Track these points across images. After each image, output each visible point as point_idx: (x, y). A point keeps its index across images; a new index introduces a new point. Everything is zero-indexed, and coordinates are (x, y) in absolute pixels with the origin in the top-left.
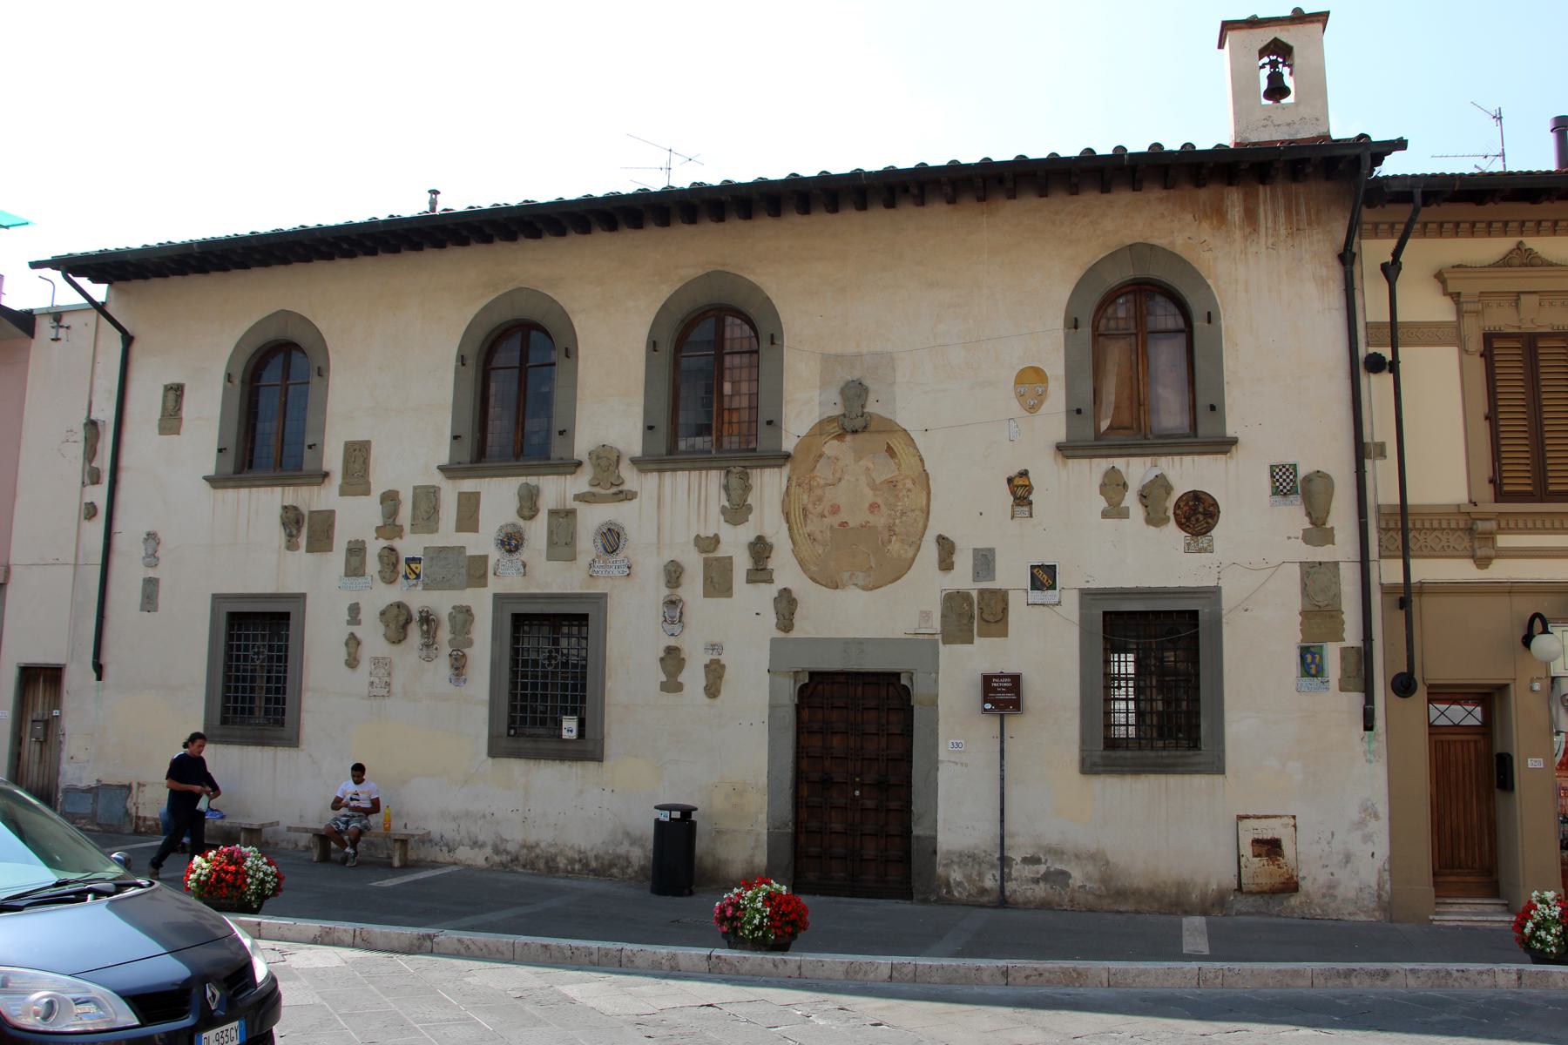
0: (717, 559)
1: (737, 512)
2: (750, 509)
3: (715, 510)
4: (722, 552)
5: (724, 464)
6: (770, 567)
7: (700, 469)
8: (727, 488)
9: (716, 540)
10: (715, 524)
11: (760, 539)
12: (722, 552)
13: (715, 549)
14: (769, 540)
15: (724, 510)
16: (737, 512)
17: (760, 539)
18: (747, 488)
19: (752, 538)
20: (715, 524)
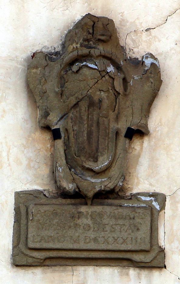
6: (142, 182)
11: (95, 35)
14: (137, 46)
17: (95, 35)
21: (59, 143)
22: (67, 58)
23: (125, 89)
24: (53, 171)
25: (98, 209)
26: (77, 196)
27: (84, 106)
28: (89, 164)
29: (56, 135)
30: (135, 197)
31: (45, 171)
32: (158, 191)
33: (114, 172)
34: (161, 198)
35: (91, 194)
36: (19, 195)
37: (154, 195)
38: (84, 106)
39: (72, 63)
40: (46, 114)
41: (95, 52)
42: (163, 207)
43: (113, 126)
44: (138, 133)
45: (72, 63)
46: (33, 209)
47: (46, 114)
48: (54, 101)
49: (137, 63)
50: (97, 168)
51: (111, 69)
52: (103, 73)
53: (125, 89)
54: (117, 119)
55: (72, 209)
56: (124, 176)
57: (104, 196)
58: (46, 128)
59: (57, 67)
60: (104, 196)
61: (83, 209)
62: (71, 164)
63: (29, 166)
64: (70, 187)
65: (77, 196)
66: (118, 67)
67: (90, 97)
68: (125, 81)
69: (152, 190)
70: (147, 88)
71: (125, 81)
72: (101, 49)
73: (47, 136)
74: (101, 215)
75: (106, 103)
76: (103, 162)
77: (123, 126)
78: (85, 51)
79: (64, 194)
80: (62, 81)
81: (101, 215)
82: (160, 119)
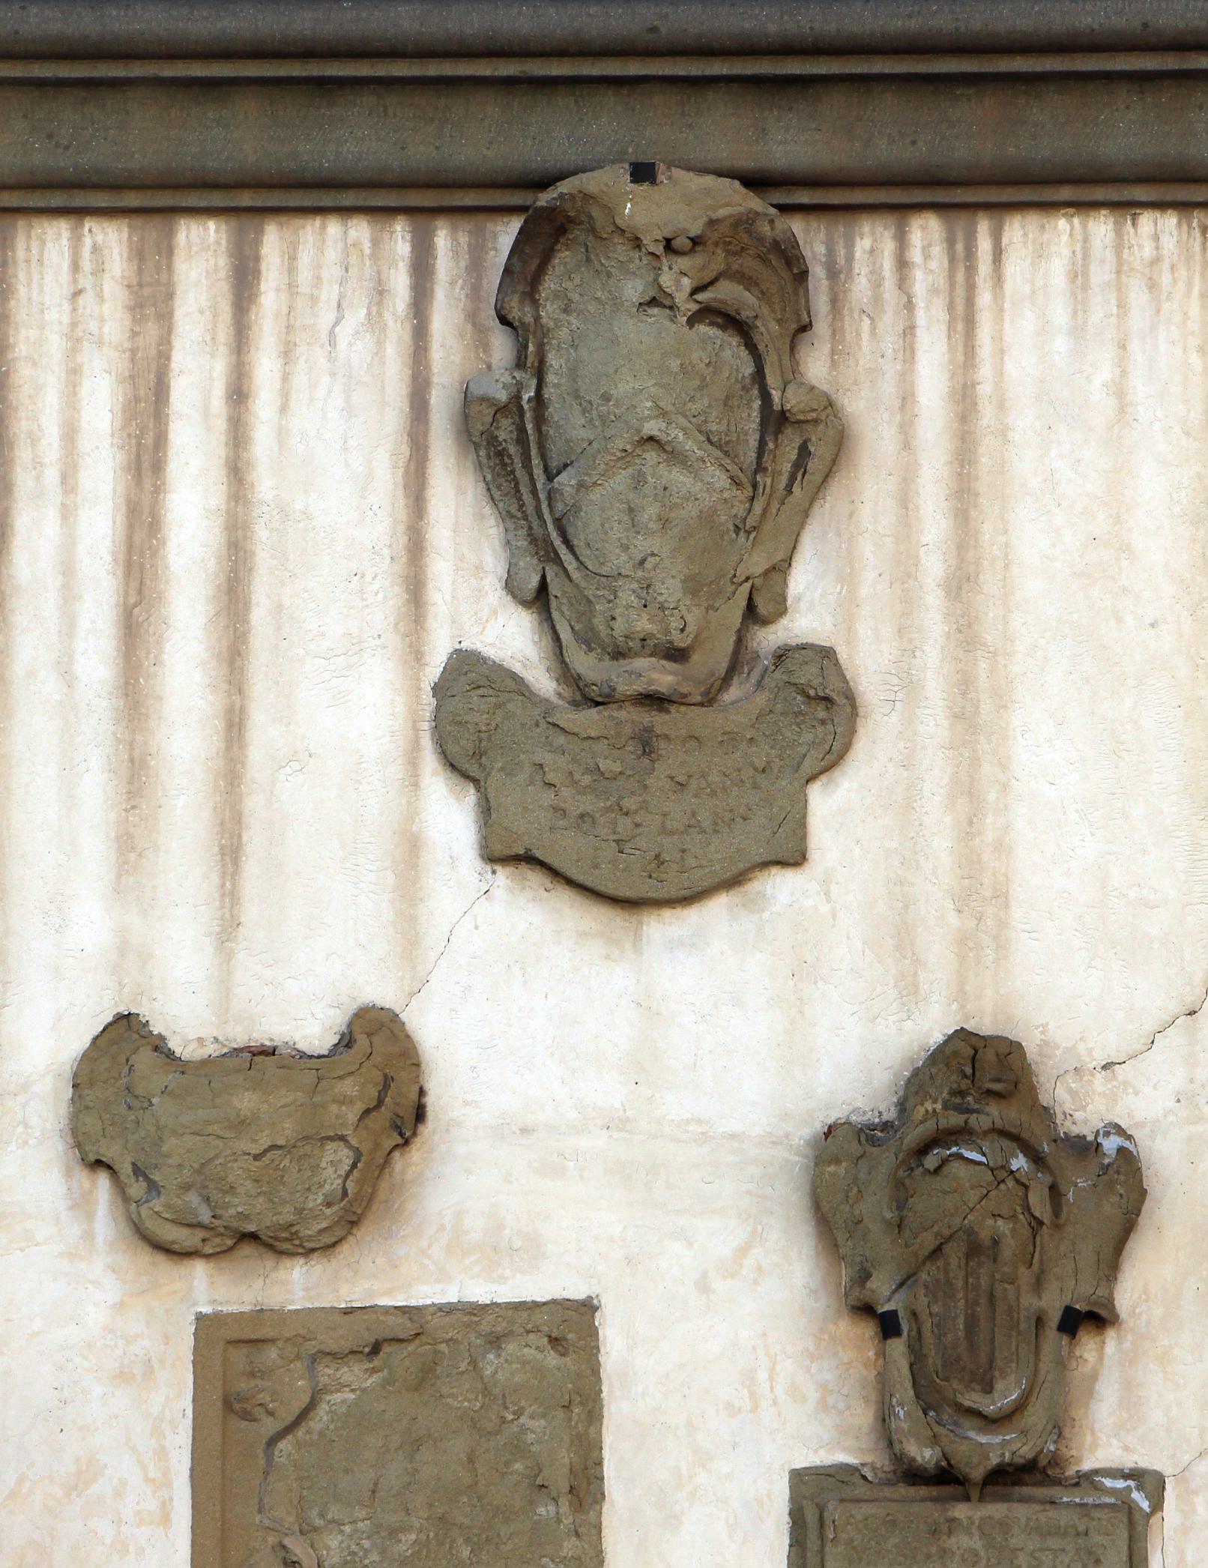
0: (391, 1340)
1: (651, 737)
2: (819, 708)
3: (348, 718)
4: (460, 1239)
5: (485, 137)
6: (1105, 1443)
7: (149, 198)
8: (515, 446)
9: (371, 1098)
10: (348, 889)
11: (977, 1081)
12: (460, 1239)
13: (357, 1209)
14: (1082, 1107)
15: (470, 721)
16: (651, 737)
17: (977, 1081)
18: (791, 450)
19: (856, 1053)
20: (348, 889)
21: (898, 1347)
22: (912, 1137)
23: (1057, 1211)
24: (884, 1418)
25: (996, 1510)
26: (945, 1479)
27: (955, 1254)
28: (972, 1399)
29: (888, 1326)
30: (1088, 1480)
31: (864, 1416)
32: (1144, 1463)
33: (1035, 1417)
34: (1152, 1483)
35: (977, 1474)
36: (798, 1477)
37: (1136, 1475)
38: (955, 1254)
39: (923, 1150)
40: (863, 1276)
41: (980, 1122)
42: (1158, 1505)
43: (1029, 1302)
44: (1089, 1319)
45: (923, 1150)
46: (834, 1511)
47: (863, 1276)
48: (881, 1243)
49: (1084, 1148)
50: (992, 1406)
51: (1019, 1162)
52: (1000, 1173)
53: (1057, 1211)
54: (1038, 1286)
55: (933, 1511)
56: (1058, 1430)
57: (1009, 1478)
58: (865, 1310)
59: (886, 1160)
60: (1009, 1478)
61: (961, 1511)
62: (929, 1397)
63: (823, 1405)
64: (925, 1455)
65: (945, 1479)
66: (1037, 1159)
67: (970, 1233)
68: (1055, 1192)
69: (1129, 1462)
70: (1110, 1208)
71: (1055, 1192)
72: (994, 1113)
73: (868, 1330)
74: (1004, 1526)
75: (1009, 1247)
76: (1006, 1394)
77: (1053, 1303)
78: (955, 1120)
79: (912, 1475)
80: (901, 1194)
81: (1004, 1526)
82: (1145, 1282)
